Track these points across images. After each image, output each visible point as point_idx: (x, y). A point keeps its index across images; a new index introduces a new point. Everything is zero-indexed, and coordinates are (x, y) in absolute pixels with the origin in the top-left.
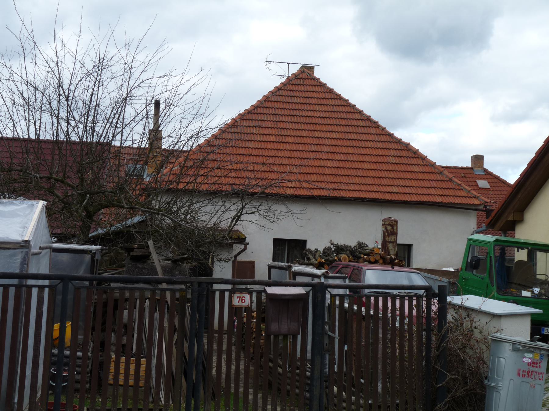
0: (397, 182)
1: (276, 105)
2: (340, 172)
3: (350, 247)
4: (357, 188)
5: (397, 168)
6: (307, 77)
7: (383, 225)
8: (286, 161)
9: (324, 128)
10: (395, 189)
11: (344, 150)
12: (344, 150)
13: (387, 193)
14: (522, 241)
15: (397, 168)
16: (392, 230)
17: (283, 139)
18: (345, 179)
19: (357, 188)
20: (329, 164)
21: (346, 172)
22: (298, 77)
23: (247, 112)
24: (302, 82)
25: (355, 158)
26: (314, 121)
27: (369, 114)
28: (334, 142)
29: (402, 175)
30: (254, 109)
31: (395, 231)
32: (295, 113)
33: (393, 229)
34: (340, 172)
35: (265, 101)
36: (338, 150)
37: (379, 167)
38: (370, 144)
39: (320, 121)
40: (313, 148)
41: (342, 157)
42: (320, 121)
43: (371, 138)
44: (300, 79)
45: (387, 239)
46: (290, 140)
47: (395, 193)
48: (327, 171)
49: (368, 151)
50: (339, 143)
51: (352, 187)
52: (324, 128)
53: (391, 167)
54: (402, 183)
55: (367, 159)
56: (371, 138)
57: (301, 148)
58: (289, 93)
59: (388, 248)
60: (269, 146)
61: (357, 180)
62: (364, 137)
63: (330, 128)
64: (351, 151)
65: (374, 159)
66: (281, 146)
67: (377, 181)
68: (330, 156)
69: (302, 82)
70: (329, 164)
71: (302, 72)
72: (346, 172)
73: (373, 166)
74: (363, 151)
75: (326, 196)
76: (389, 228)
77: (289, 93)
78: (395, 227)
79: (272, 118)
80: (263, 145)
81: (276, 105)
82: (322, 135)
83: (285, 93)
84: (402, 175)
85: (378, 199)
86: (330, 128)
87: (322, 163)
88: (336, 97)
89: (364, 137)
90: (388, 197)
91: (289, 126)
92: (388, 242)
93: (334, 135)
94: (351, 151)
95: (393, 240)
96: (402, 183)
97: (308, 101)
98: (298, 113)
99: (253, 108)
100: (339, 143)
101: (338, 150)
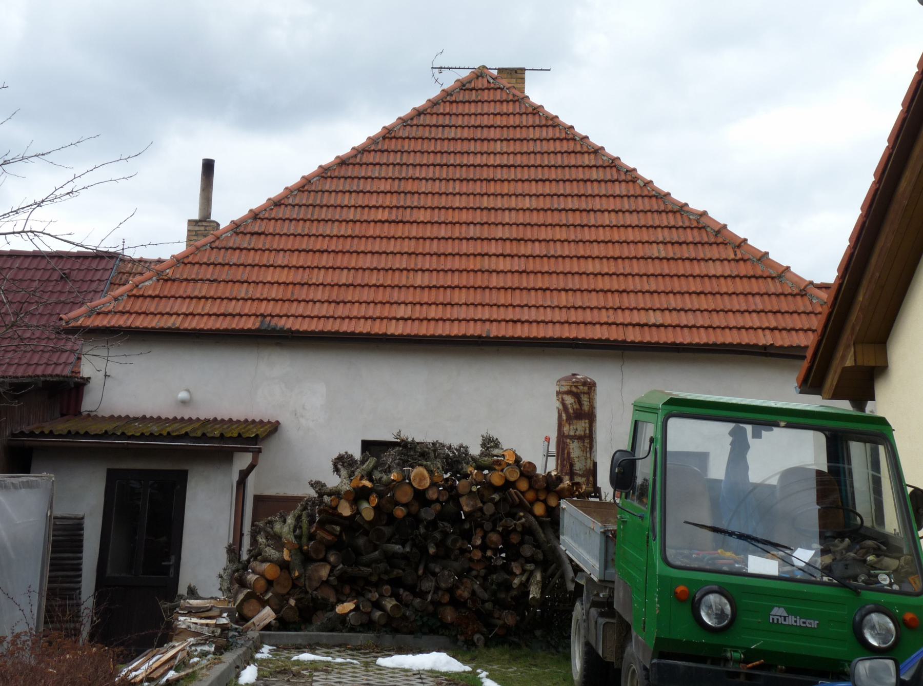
0: (657, 301)
1: (407, 146)
2: (525, 282)
3: (450, 448)
4: (558, 316)
5: (666, 268)
6: (486, 85)
7: (558, 393)
8: (403, 262)
9: (506, 188)
10: (653, 317)
11: (544, 234)
12: (544, 234)
13: (634, 325)
14: (721, 355)
15: (666, 268)
16: (576, 406)
17: (408, 215)
18: (533, 298)
19: (558, 316)
20: (502, 264)
21: (540, 282)
22: (468, 86)
23: (338, 161)
24: (473, 96)
25: (567, 250)
26: (486, 173)
27: (615, 154)
28: (521, 218)
29: (677, 285)
30: (356, 156)
31: (586, 407)
32: (445, 159)
33: (580, 402)
34: (525, 282)
35: (384, 138)
36: (529, 233)
37: (621, 267)
38: (606, 219)
39: (499, 174)
40: (472, 231)
41: (538, 249)
42: (499, 174)
43: (612, 204)
44: (471, 90)
45: (566, 429)
46: (422, 216)
47: (654, 325)
48: (495, 281)
49: (602, 235)
50: (535, 218)
51: (549, 315)
52: (506, 188)
53: (651, 268)
54: (673, 302)
55: (596, 250)
56: (612, 204)
57: (443, 232)
58: (441, 120)
59: (569, 453)
60: (371, 230)
61: (563, 299)
62: (597, 204)
63: (519, 188)
64: (560, 234)
65: (612, 251)
66: (399, 231)
67: (613, 300)
68: (508, 248)
69: (473, 96)
70: (502, 264)
71: (478, 77)
72: (540, 282)
73: (606, 267)
74: (587, 234)
75: (480, 337)
76: (569, 400)
77: (441, 120)
78: (585, 399)
79: (390, 172)
80: (358, 230)
81: (407, 146)
82: (499, 203)
83: (434, 120)
84: (677, 285)
85: (607, 340)
86: (519, 188)
87: (486, 263)
88: (544, 122)
89: (597, 204)
90: (633, 335)
91: (423, 187)
92: (569, 437)
93: (527, 203)
94: (560, 234)
95: (580, 432)
96: (673, 302)
97: (479, 134)
98: (451, 160)
99: (355, 152)
100: (535, 218)
101: (529, 233)
